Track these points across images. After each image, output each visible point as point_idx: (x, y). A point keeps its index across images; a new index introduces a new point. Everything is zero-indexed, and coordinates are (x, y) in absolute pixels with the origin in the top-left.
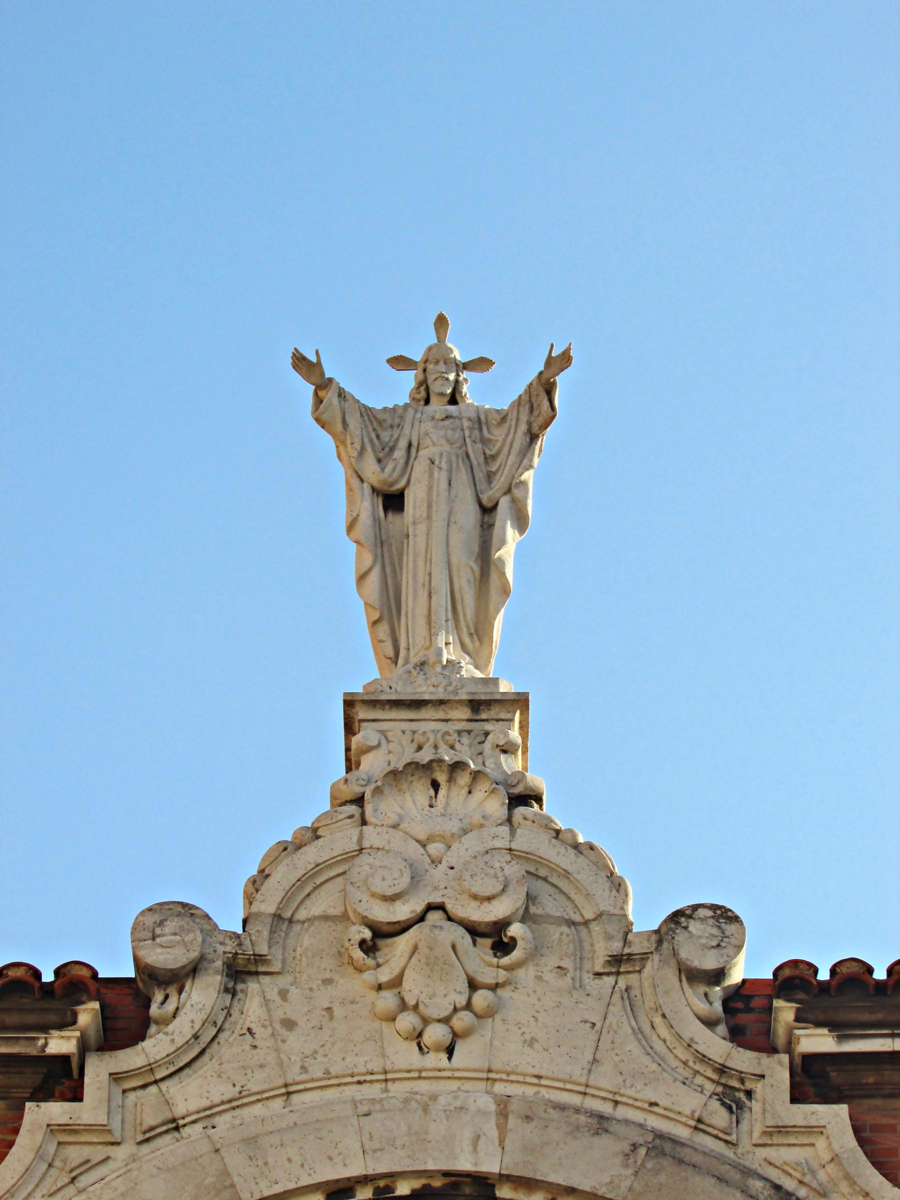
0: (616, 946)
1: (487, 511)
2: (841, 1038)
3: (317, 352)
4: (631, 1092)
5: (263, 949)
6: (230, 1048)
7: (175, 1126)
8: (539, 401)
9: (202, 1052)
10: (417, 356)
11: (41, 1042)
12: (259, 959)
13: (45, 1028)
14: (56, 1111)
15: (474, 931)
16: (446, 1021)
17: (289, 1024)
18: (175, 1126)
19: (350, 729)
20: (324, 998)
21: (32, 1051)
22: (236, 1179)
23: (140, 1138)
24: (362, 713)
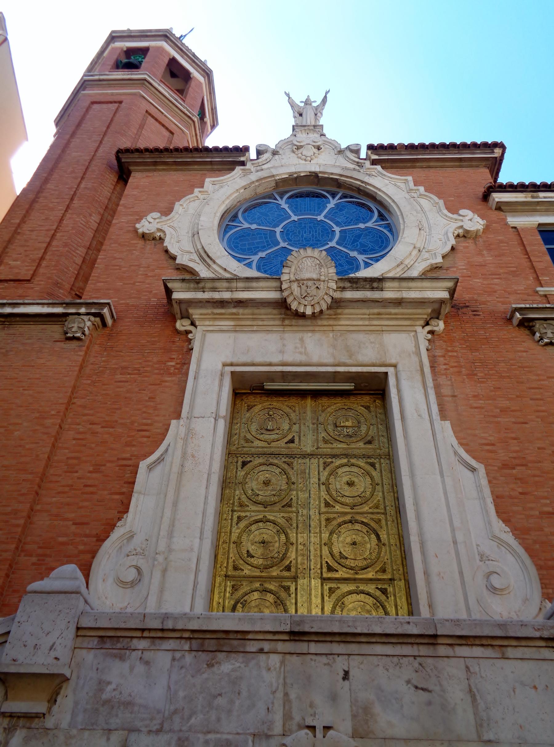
0: (339, 150)
1: (316, 115)
7: (262, 170)
13: (240, 157)
14: (242, 167)
15: (314, 146)
18: (262, 170)
19: (293, 130)
20: (289, 156)
24: (295, 128)
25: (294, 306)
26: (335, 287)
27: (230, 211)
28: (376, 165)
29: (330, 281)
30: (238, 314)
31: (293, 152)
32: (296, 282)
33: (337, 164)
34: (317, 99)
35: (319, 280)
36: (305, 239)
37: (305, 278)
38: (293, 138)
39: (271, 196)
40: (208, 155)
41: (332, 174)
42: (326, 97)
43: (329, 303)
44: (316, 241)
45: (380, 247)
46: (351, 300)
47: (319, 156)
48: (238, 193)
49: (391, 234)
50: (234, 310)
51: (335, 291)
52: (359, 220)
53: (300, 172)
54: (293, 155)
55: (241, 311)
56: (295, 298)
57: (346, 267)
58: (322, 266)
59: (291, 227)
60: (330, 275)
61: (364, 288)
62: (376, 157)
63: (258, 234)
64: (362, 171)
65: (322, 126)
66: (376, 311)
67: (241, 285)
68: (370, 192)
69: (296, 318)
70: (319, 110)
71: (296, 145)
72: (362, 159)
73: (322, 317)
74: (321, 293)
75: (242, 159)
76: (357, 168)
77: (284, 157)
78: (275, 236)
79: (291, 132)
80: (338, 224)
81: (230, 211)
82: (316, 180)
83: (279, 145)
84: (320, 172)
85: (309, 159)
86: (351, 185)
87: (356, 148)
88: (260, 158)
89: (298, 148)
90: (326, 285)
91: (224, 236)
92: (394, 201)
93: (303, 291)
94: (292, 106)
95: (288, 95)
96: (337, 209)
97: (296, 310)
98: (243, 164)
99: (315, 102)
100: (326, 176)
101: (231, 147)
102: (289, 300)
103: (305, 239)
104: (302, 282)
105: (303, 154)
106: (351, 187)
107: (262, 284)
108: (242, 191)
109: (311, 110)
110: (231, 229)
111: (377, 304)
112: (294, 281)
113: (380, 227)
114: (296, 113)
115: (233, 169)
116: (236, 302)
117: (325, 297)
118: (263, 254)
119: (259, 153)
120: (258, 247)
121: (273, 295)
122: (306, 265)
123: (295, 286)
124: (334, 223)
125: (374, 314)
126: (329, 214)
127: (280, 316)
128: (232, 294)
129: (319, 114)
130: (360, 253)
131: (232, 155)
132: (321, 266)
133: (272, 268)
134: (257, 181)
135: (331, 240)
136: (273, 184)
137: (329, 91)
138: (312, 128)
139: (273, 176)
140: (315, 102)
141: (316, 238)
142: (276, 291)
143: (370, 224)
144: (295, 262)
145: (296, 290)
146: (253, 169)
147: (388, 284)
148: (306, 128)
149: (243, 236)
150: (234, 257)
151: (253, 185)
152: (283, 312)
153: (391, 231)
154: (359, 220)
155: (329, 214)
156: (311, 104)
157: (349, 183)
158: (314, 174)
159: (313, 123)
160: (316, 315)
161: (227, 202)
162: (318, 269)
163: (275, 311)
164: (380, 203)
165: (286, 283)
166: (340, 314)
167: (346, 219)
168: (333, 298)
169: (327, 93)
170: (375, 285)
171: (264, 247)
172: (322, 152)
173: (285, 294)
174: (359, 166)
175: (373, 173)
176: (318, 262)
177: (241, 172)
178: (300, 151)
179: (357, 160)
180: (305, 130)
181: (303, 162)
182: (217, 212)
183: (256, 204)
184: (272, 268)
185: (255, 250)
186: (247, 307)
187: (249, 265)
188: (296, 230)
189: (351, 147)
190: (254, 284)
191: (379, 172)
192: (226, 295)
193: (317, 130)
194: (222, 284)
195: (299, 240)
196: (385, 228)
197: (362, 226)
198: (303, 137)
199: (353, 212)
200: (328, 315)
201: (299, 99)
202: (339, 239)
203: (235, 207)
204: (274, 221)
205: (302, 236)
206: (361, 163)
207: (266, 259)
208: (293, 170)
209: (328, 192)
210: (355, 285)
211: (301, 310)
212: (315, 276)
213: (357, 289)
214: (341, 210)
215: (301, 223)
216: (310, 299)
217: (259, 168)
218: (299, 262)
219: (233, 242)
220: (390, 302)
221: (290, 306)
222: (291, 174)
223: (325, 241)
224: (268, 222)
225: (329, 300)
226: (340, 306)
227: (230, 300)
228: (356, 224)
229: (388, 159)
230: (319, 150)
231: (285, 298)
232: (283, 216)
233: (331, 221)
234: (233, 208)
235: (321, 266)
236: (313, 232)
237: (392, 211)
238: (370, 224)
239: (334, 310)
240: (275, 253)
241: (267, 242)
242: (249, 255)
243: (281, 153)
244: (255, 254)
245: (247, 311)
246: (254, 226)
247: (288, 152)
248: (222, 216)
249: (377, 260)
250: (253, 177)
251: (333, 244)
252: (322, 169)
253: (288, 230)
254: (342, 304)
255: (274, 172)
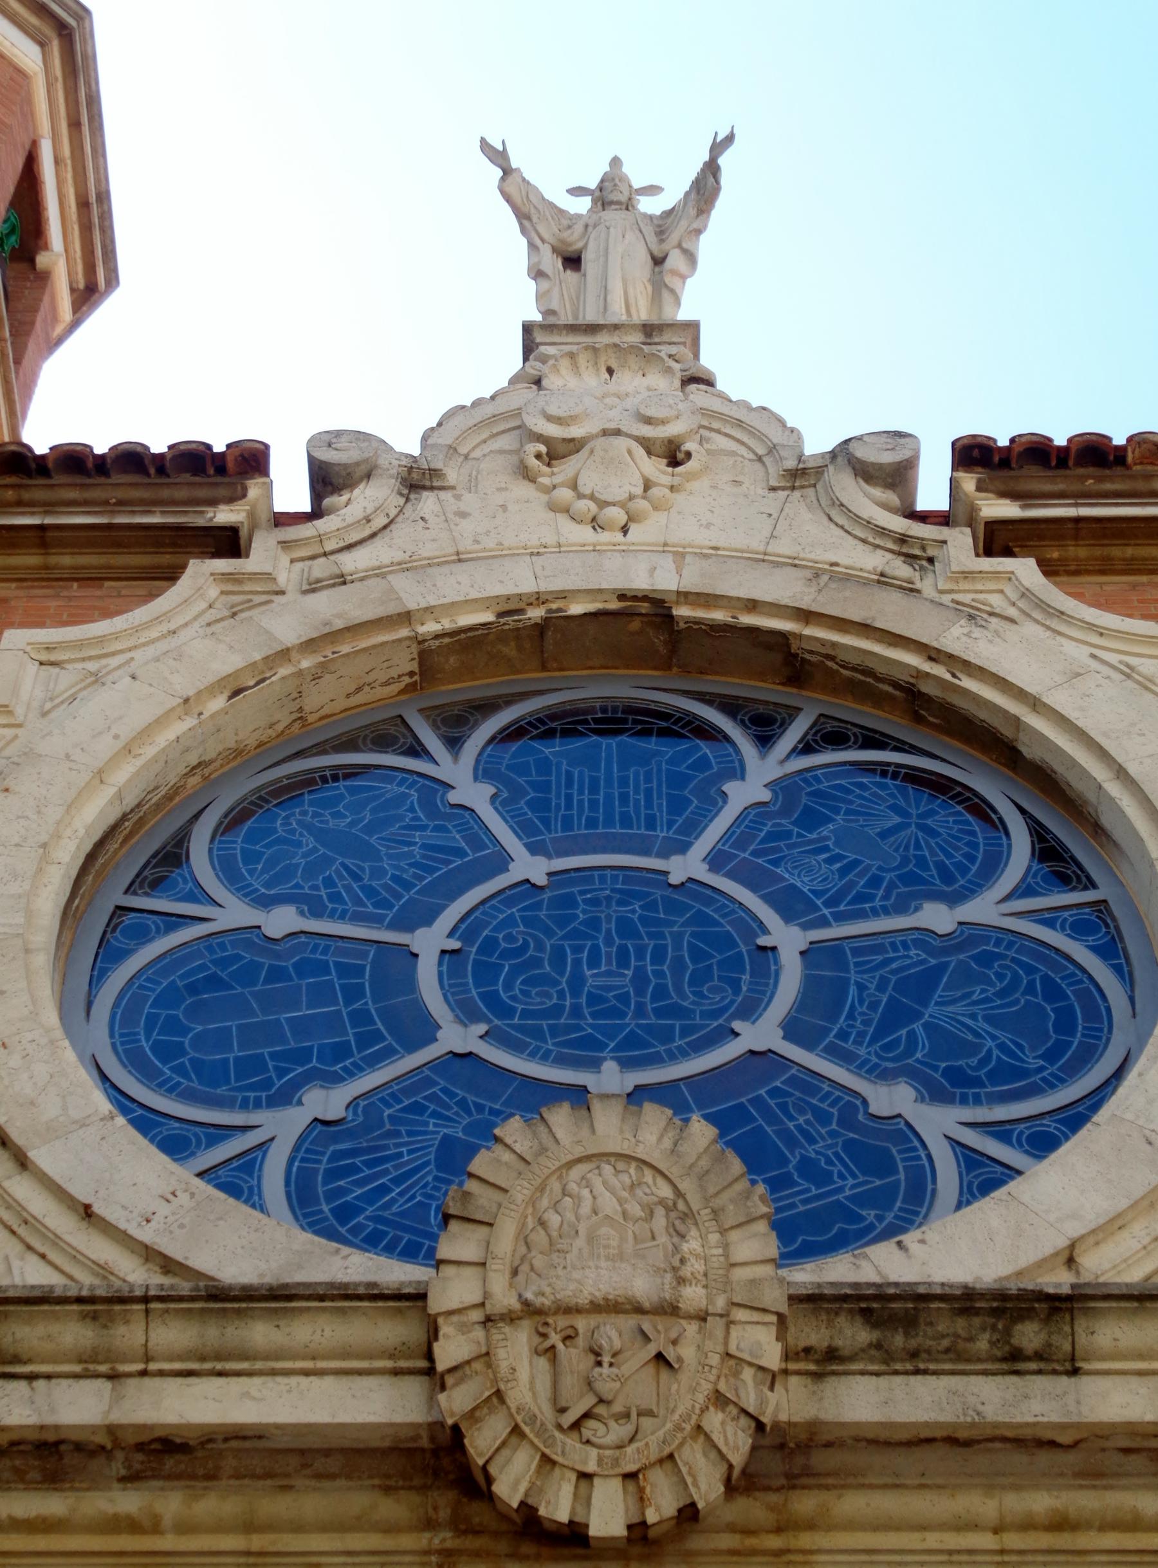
0: (791, 464)
1: (658, 261)
2: (1023, 507)
3: (503, 142)
4: (812, 556)
5: (438, 465)
6: (402, 534)
7: (342, 580)
8: (706, 187)
9: (373, 535)
10: (593, 184)
11: (210, 515)
12: (434, 473)
13: (213, 502)
14: (222, 565)
15: (648, 446)
16: (622, 505)
17: (463, 515)
18: (342, 580)
19: (529, 349)
21: (201, 522)
22: (402, 594)
23: (305, 587)
24: (539, 337)
25: (511, 1483)
26: (772, 1358)
27: (141, 822)
28: (1008, 552)
29: (740, 1315)
30: (155, 1527)
31: (526, 474)
32: (526, 1325)
33: (783, 547)
34: (667, 180)
35: (670, 1310)
36: (593, 999)
37: (583, 1300)
38: (527, 393)
39: (391, 735)
40: (26, 495)
41: (752, 605)
42: (711, 169)
43: (738, 1459)
44: (659, 1013)
45: (1051, 1056)
46: (884, 1435)
47: (679, 498)
48: (190, 722)
49: (1118, 969)
50: (128, 1502)
51: (772, 1378)
52: (924, 882)
53: (563, 595)
54: (524, 490)
55: (170, 1503)
56: (516, 1431)
57: (848, 1187)
58: (688, 1216)
59: (510, 921)
60: (739, 1274)
61: (957, 1358)
62: (1007, 509)
63: (302, 968)
64: (926, 586)
65: (692, 328)
66: (1041, 1502)
67: (172, 1335)
68: (983, 715)
69: (527, 1548)
70: (674, 238)
71: (540, 438)
72: (924, 517)
73: (697, 1542)
74: (686, 1394)
75: (224, 515)
76: (901, 570)
77: (469, 501)
78: (410, 983)
79: (514, 361)
80: (791, 906)
81: (141, 822)
82: (659, 640)
83: (446, 438)
84: (685, 596)
85: (617, 515)
86: (869, 672)
87: (887, 458)
88: (329, 512)
89: (555, 452)
90: (714, 1347)
91: (97, 977)
92: (1121, 773)
93: (570, 1384)
94: (523, 216)
95: (498, 156)
96: (785, 812)
97: (527, 1510)
98: (229, 543)
99: (652, 190)
100: (719, 615)
101: (158, 446)
102: (481, 1443)
103: (593, 999)
104: (562, 1322)
105: (585, 487)
106: (863, 682)
107: (310, 1331)
108: (218, 703)
109: (631, 236)
110: (143, 935)
111: (1044, 1458)
112: (510, 1318)
113: (1049, 923)
114: (546, 250)
115: (172, 575)
116: (140, 1447)
117: (714, 1421)
118: (328, 1102)
119: (326, 480)
120: (302, 1056)
121: (378, 1405)
122: (585, 1209)
123: (516, 1349)
124: (768, 899)
125: (1028, 1525)
126: (741, 844)
127: (423, 1540)
128: (117, 1399)
129: (675, 260)
130: (934, 1094)
131: (165, 493)
132: (681, 1217)
133: (383, 1190)
134: (309, 645)
135: (751, 1010)
136: (406, 662)
137: (730, 139)
138: (636, 338)
139: (406, 617)
140: (652, 190)
141: (660, 992)
142: (396, 1372)
143: (984, 909)
144: (521, 1192)
145: (524, 1374)
146: (287, 574)
147: (1108, 1333)
148: (603, 339)
149: (214, 982)
150: (145, 1121)
151: (283, 671)
152: (444, 1514)
153: (1112, 950)
154: (923, 881)
155: (741, 844)
156: (628, 205)
157: (855, 660)
158: (645, 607)
159: (643, 314)
160: (652, 1533)
161: (122, 775)
162: (663, 1239)
163: (391, 1508)
164: (1044, 780)
165: (464, 1328)
166: (811, 1526)
167: (844, 872)
168: (760, 1426)
169: (719, 147)
170: (1029, 1335)
171: (341, 1051)
172: (691, 477)
173: (456, 1401)
174: (910, 558)
175: (996, 601)
176: (665, 1191)
177: (213, 592)
178: (566, 469)
179: (898, 524)
180: (595, 350)
181: (585, 534)
182: (57, 836)
183: (301, 785)
184: (383, 1190)
185: (281, 1073)
186: (211, 1477)
187: (237, 1180)
188: (540, 947)
189: (860, 452)
190: (260, 1333)
191: (1026, 594)
192: (79, 1406)
193: (664, 350)
194: (55, 1328)
195: (557, 1011)
196: (1079, 929)
197: (937, 917)
198: (581, 393)
199: (884, 835)
200: (732, 1528)
201: (561, 177)
202: (804, 1003)
203: (169, 798)
204: (407, 886)
205: (577, 983)
206: (923, 544)
207: (351, 1134)
208: (520, 580)
209: (730, 706)
210: (898, 1340)
211: (558, 1507)
212: (642, 1285)
213: (917, 1362)
214: (811, 819)
215: (568, 901)
216: (618, 1432)
217: (321, 568)
218: (542, 1189)
219: (152, 1020)
220: (1127, 1451)
221: (489, 1480)
222: (510, 608)
223: (715, 1014)
224: (370, 892)
225: (737, 1442)
226: (808, 1472)
227: (102, 1439)
228: (901, 908)
229: (1078, 520)
230: (674, 462)
231: (456, 1428)
232: (459, 852)
233: (753, 887)
234: (158, 806)
235: (681, 1217)
236: (640, 956)
237: (1117, 834)
238: (984, 909)
239: (774, 1498)
240: (406, 1092)
241: (361, 1017)
242: (245, 1105)
243: (452, 476)
244: (285, 1097)
245: (213, 1504)
246: (282, 921)
247: (494, 473)
248: (91, 857)
249: (1042, 1143)
250: (287, 623)
251: (761, 1033)
252: (692, 579)
253: (489, 945)
254: (821, 1460)
255: (412, 593)
